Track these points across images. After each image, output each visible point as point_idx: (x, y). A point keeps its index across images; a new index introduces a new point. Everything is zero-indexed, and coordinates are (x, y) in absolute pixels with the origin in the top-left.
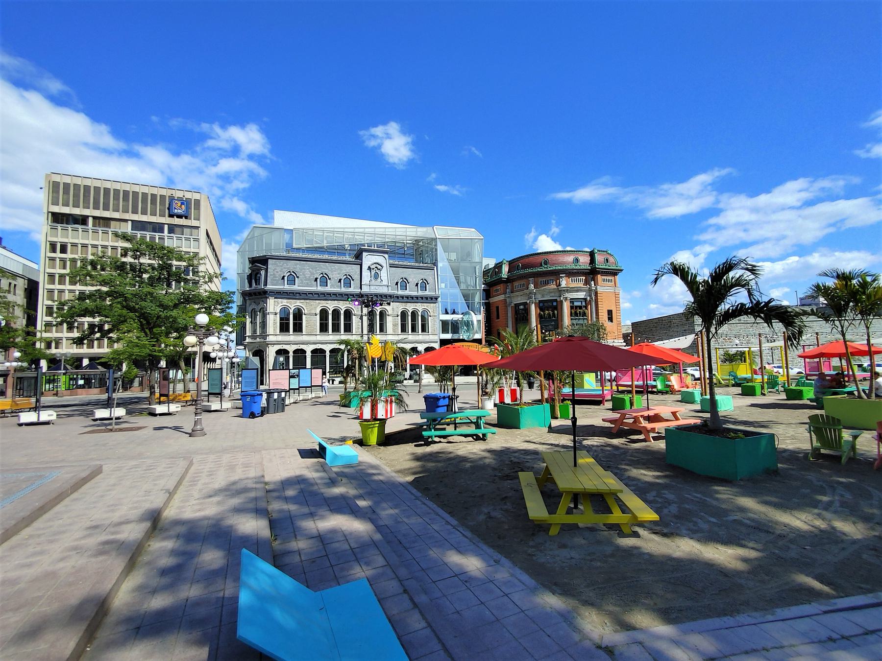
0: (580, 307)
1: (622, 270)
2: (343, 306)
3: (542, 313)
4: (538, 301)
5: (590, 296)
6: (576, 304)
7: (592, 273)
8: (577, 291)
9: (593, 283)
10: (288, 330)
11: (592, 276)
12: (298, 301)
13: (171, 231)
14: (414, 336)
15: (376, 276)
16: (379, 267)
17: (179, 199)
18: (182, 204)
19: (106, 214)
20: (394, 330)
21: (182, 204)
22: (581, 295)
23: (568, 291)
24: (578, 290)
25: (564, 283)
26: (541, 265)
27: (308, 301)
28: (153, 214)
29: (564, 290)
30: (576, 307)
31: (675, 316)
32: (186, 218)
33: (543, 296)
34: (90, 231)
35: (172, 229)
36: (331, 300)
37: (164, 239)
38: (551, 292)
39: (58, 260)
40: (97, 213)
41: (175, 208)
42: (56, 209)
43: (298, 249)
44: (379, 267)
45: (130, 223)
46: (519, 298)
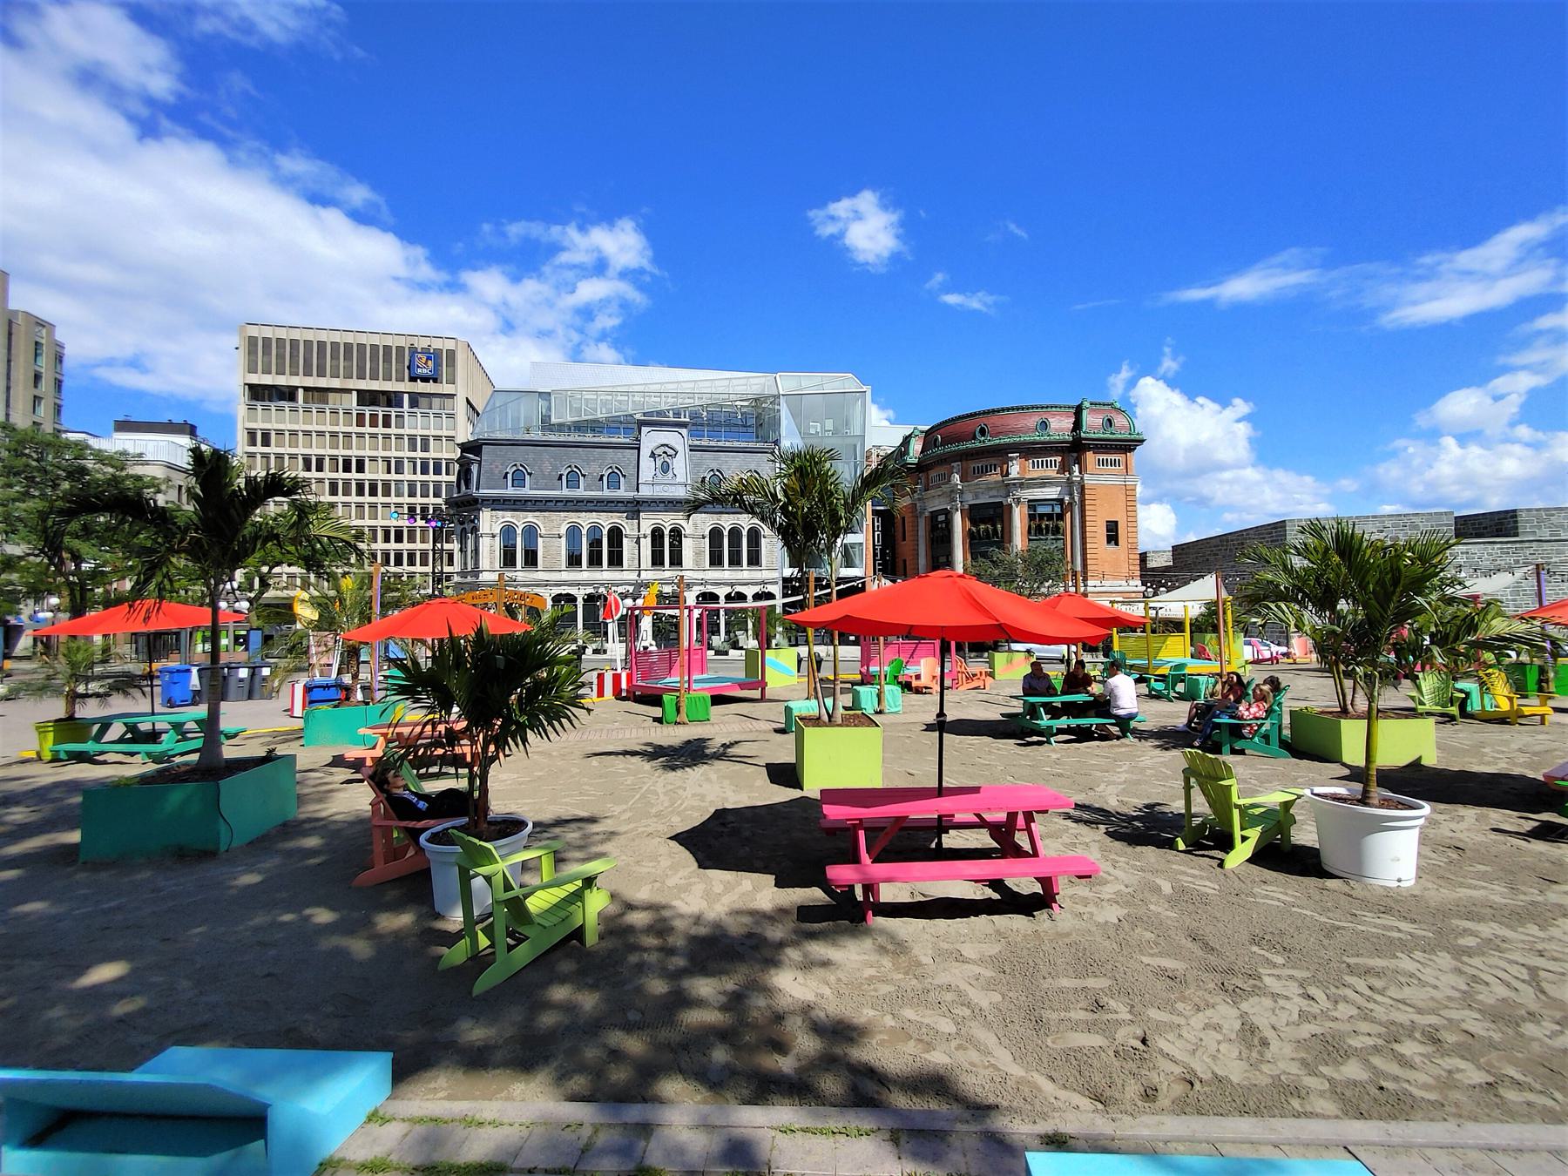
0: (1050, 517)
1: (1142, 441)
2: (606, 521)
3: (974, 529)
4: (967, 507)
5: (1071, 494)
6: (1041, 510)
7: (1075, 449)
8: (1043, 485)
9: (1076, 468)
10: (600, 563)
11: (1075, 455)
12: (530, 514)
13: (414, 403)
14: (733, 573)
15: (665, 468)
16: (671, 452)
17: (425, 351)
18: (429, 358)
19: (322, 383)
20: (697, 563)
21: (429, 358)
22: (1052, 493)
23: (1022, 486)
24: (1044, 483)
25: (1015, 470)
26: (974, 438)
27: (546, 514)
28: (388, 378)
29: (1014, 484)
30: (1042, 516)
31: (1251, 532)
32: (435, 381)
33: (976, 496)
34: (301, 410)
35: (415, 400)
36: (586, 511)
37: (403, 416)
38: (992, 489)
39: (259, 456)
40: (311, 382)
41: (418, 367)
42: (255, 379)
43: (561, 427)
44: (671, 452)
45: (355, 393)
46: (937, 502)
